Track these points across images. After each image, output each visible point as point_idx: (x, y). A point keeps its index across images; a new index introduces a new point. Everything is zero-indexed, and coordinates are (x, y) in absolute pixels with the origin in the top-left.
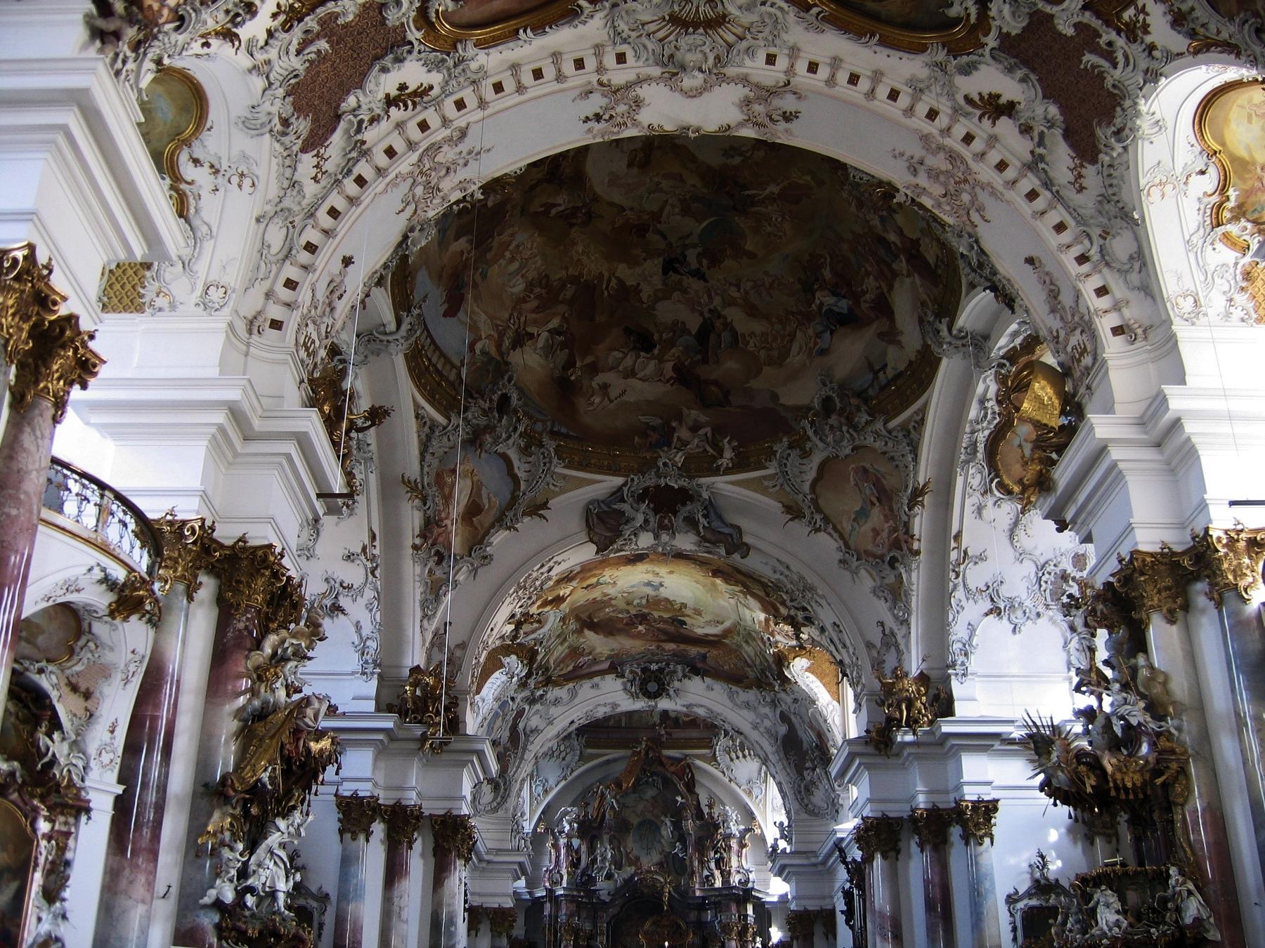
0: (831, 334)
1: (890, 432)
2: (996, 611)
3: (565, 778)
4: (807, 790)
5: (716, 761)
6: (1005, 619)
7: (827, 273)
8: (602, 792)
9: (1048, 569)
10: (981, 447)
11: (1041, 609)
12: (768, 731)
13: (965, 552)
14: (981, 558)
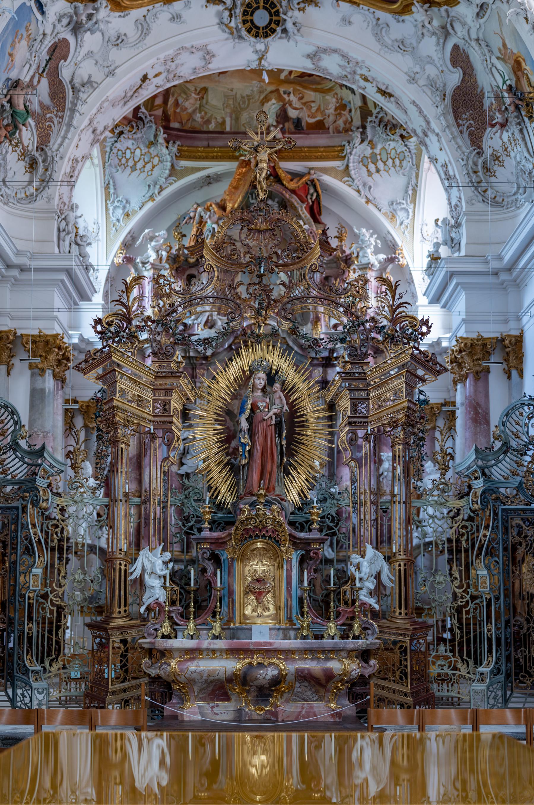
3: (152, 198)
4: (486, 169)
5: (349, 176)
8: (201, 217)
12: (432, 84)
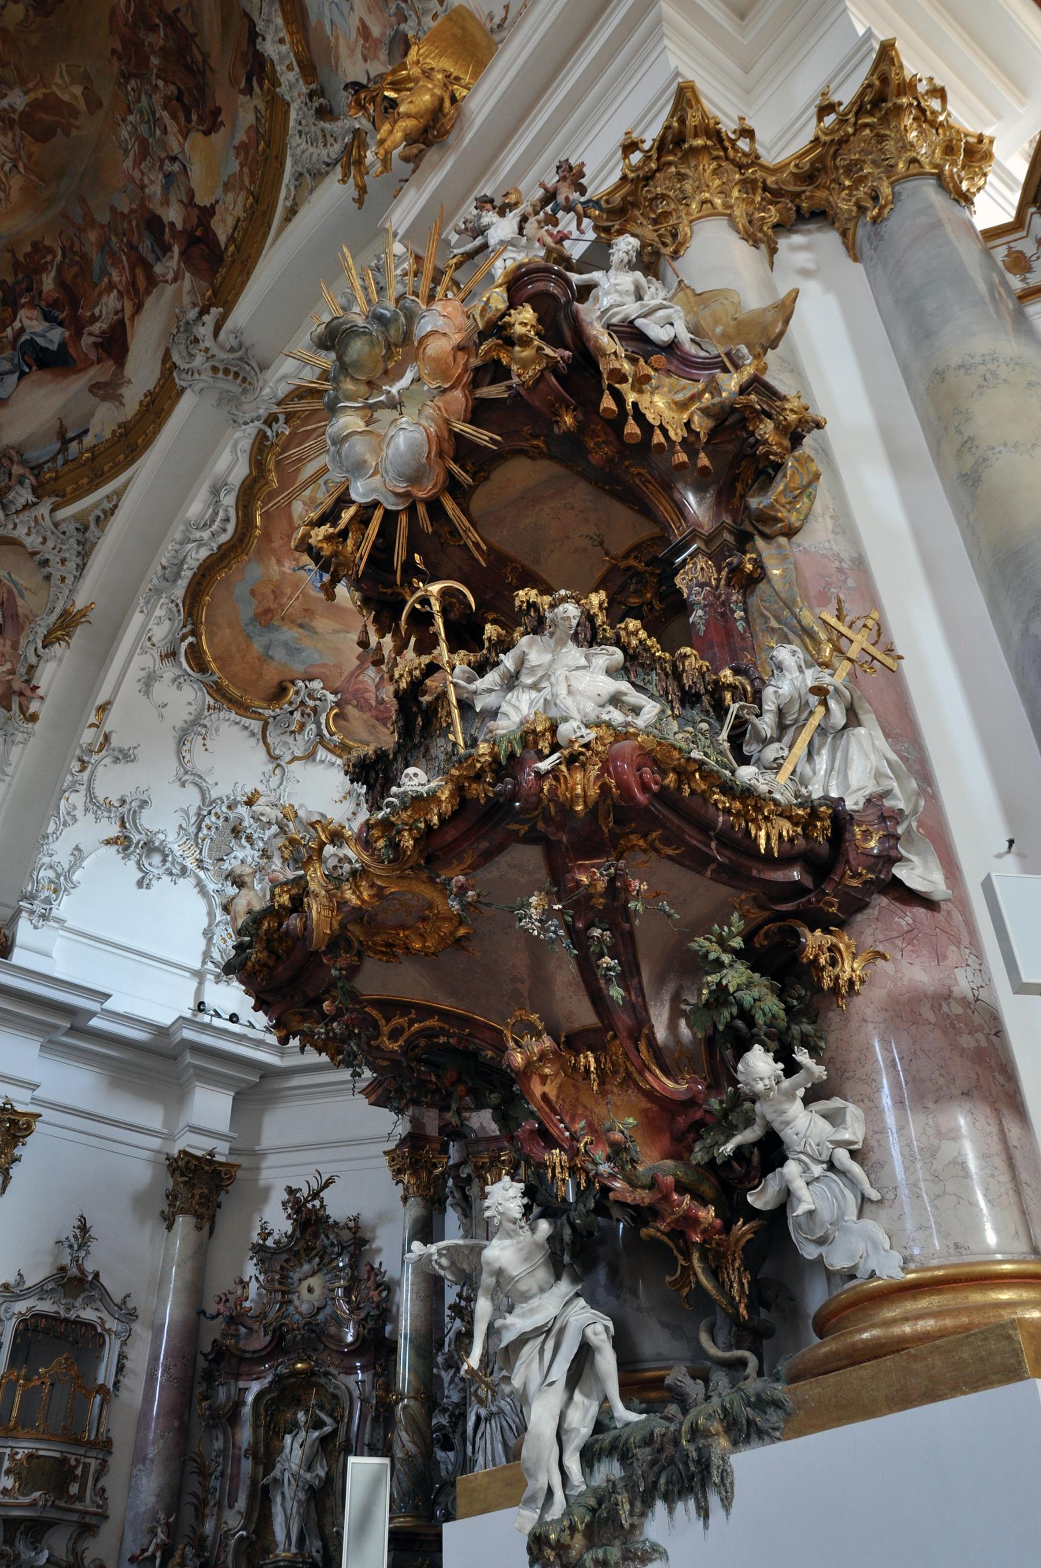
0: (20, 378)
1: (56, 525)
2: (122, 843)
6: (134, 858)
7: (48, 282)
9: (218, 810)
10: (187, 575)
11: (190, 864)
13: (107, 737)
14: (125, 756)
